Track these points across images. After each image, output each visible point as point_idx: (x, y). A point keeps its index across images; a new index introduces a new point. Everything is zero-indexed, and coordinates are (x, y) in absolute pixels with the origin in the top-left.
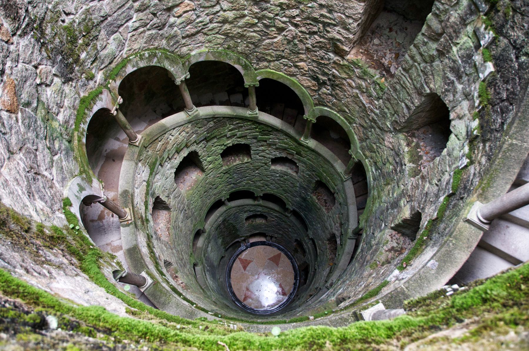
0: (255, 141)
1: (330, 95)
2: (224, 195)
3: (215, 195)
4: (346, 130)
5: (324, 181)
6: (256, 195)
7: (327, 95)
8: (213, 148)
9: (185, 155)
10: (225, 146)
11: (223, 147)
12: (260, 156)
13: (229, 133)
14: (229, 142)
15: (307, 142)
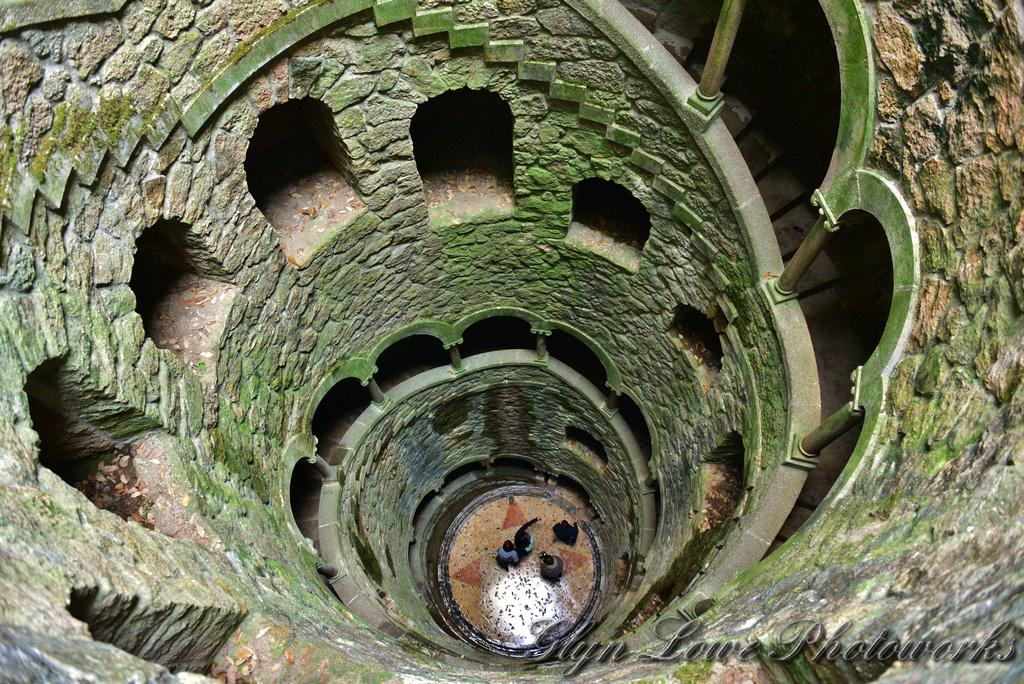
0: (666, 213)
1: (936, 129)
2: (543, 323)
3: (520, 297)
4: (898, 288)
5: (746, 441)
6: (607, 384)
7: (926, 126)
8: (559, 146)
9: (473, 85)
10: (595, 167)
11: (585, 166)
12: (659, 275)
13: (615, 126)
14: (605, 162)
15: (779, 298)
